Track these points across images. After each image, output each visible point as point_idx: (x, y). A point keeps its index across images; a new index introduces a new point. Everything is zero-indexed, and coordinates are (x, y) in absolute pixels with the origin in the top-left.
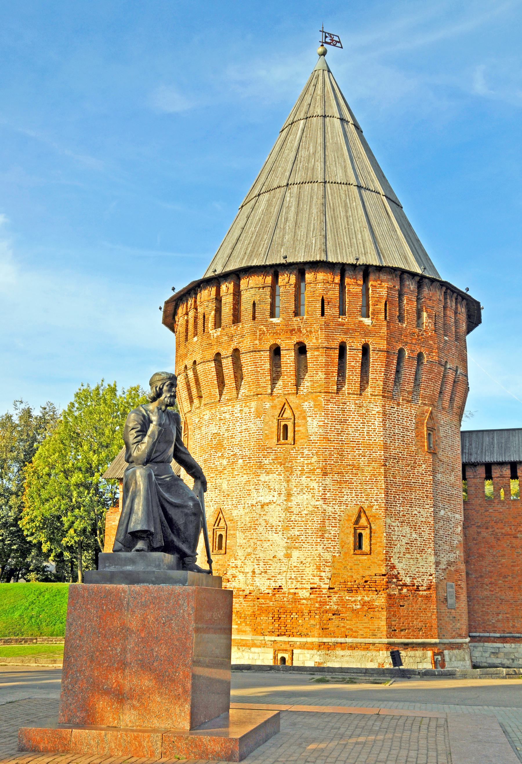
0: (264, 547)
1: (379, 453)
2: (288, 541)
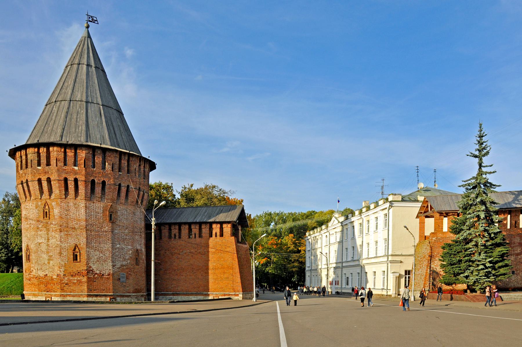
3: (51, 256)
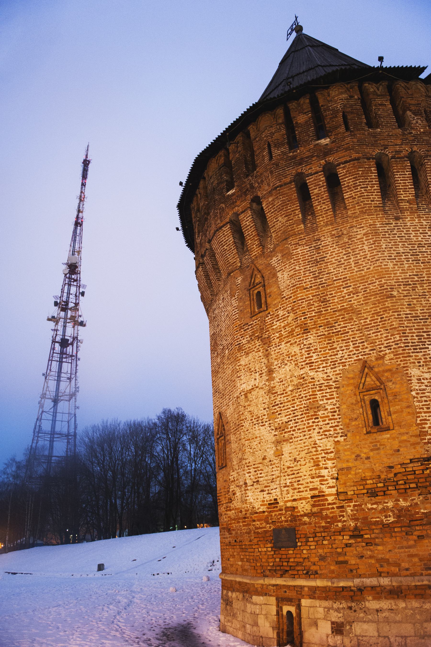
0: (253, 447)
1: (378, 283)
2: (276, 433)
3: (281, 428)
